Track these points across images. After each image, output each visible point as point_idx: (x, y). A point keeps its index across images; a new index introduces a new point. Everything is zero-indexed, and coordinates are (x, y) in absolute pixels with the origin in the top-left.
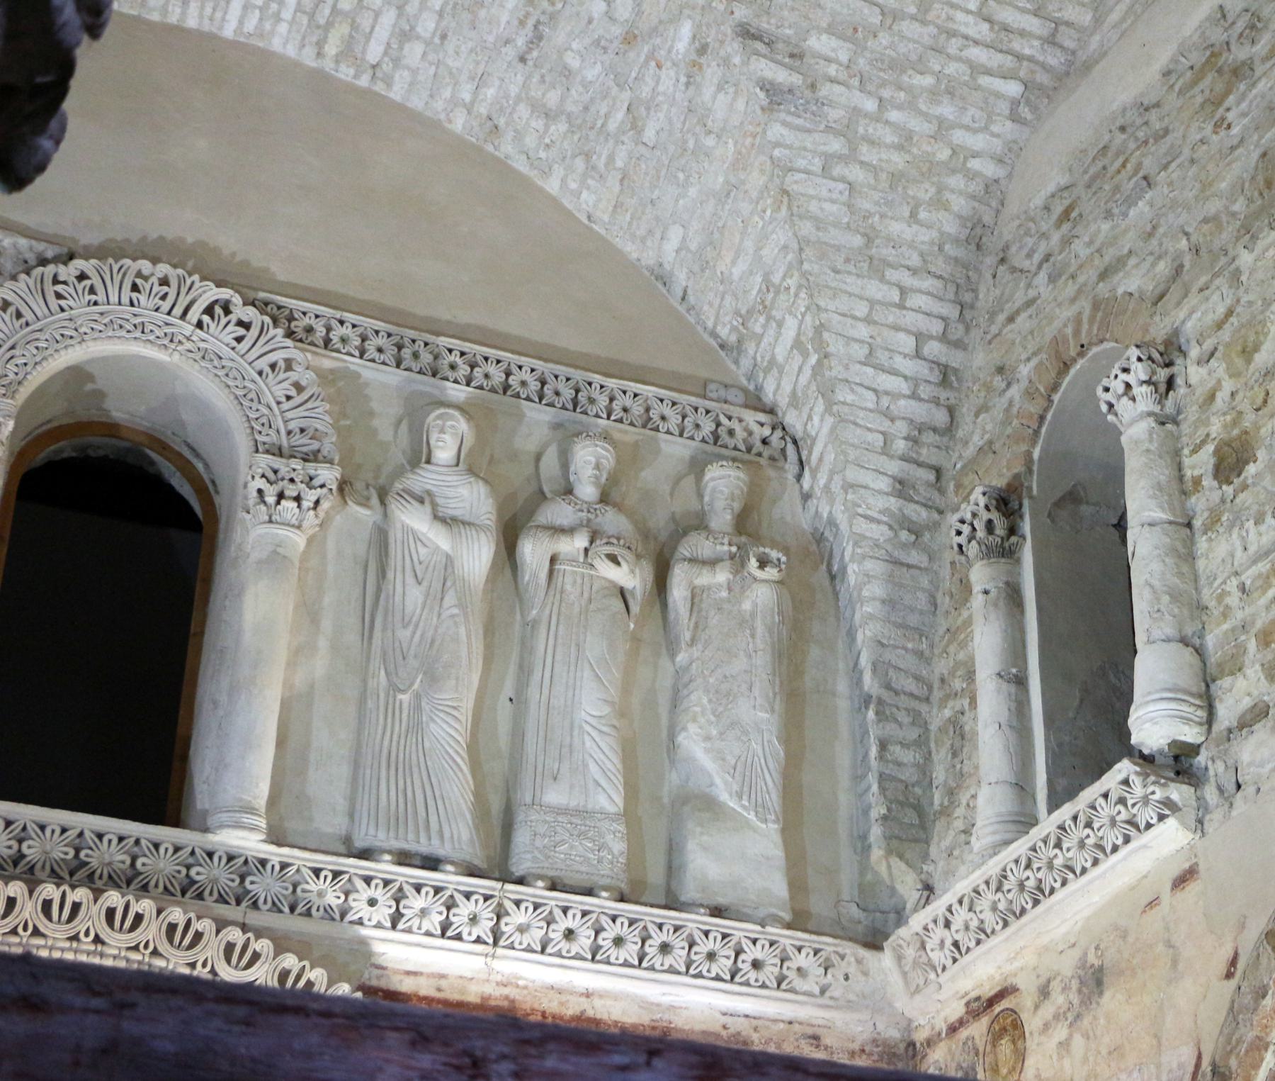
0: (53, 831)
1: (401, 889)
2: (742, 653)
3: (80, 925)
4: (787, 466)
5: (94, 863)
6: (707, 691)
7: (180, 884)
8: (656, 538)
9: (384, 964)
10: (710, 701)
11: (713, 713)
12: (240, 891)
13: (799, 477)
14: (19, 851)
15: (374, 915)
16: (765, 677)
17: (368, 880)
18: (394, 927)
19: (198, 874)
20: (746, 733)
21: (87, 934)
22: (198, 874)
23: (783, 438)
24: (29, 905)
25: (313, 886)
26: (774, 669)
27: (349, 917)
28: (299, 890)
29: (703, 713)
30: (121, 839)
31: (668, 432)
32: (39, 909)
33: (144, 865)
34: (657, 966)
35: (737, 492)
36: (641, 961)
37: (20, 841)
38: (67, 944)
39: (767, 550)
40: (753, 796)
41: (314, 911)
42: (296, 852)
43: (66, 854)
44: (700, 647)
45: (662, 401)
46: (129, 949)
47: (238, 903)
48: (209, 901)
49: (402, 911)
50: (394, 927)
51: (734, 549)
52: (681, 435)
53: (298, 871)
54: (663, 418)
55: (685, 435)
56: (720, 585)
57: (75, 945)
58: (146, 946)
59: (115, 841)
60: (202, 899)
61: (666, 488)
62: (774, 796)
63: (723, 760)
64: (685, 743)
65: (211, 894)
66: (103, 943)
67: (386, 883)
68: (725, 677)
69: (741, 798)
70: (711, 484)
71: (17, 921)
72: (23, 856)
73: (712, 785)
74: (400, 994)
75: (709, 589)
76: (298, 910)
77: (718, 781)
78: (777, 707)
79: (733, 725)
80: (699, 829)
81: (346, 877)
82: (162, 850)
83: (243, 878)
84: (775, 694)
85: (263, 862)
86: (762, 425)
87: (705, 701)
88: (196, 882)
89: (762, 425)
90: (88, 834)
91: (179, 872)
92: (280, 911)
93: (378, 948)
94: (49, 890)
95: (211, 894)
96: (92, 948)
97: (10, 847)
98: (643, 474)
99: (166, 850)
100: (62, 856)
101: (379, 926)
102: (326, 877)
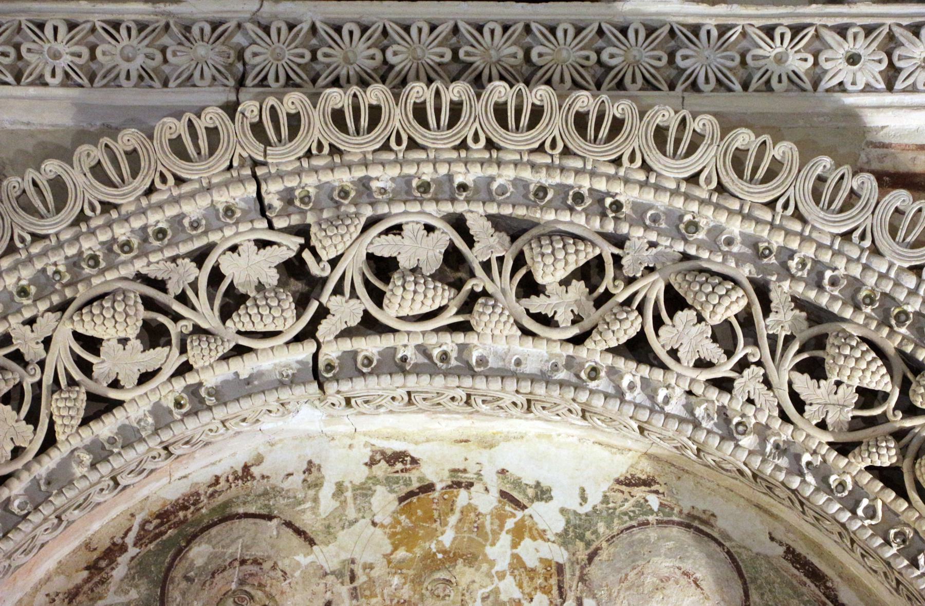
0: (420, 30)
1: (891, 37)
3: (465, 129)
5: (479, 62)
7: (593, 76)
9: (887, 141)
12: (674, 72)
14: (385, 62)
15: (859, 75)
17: (842, 31)
18: (890, 88)
19: (612, 56)
21: (476, 139)
22: (612, 56)
24: (397, 112)
25: (768, 50)
27: (825, 84)
28: (749, 59)
30: (506, 28)
32: (411, 116)
33: (540, 55)
37: (383, 51)
38: (454, 155)
41: (774, 82)
42: (736, 9)
43: (442, 56)
46: (532, 151)
47: (672, 87)
48: (633, 89)
49: (899, 64)
50: (890, 88)
53: (744, 34)
57: (463, 154)
58: (553, 145)
59: (499, 30)
60: (625, 89)
65: (634, 81)
66: (499, 149)
67: (869, 30)
71: (387, 133)
72: (392, 67)
74: (915, 175)
76: (754, 85)
81: (811, 31)
82: (560, 34)
83: (672, 56)
85: (695, 29)
88: (611, 68)
90: (463, 26)
91: (587, 58)
92: (730, 90)
93: (874, 120)
94: (418, 91)
95: (634, 81)
96: (486, 155)
97: (373, 58)
99: (566, 31)
100: (438, 59)
101: (868, 89)
102: (782, 36)
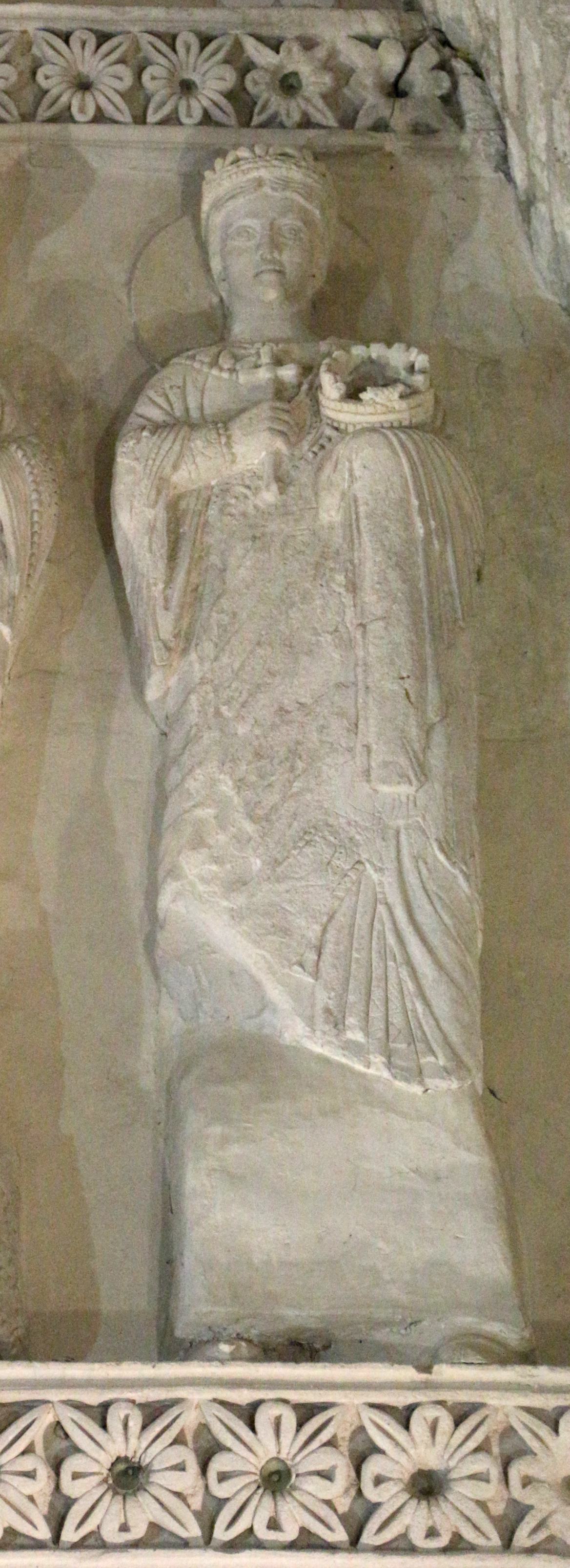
2: (327, 639)
4: (465, 142)
6: (229, 760)
8: (90, 405)
10: (240, 784)
11: (252, 817)
13: (503, 162)
16: (391, 686)
20: (347, 846)
23: (443, 66)
26: (419, 661)
29: (222, 822)
31: (100, 117)
34: (111, 1534)
35: (289, 221)
36: (57, 1523)
39: (376, 350)
40: (376, 1013)
44: (208, 648)
45: (66, 38)
51: (289, 373)
52: (140, 119)
54: (84, 86)
55: (151, 118)
56: (256, 476)
61: (117, 272)
62: (442, 1005)
63: (286, 932)
64: (180, 907)
68: (282, 711)
69: (337, 1022)
70: (218, 219)
73: (265, 1005)
75: (225, 489)
77: (275, 993)
78: (436, 758)
79: (306, 837)
80: (217, 1130)
84: (428, 731)
86: (374, 43)
87: (226, 787)
89: (374, 43)
98: (46, 246)
